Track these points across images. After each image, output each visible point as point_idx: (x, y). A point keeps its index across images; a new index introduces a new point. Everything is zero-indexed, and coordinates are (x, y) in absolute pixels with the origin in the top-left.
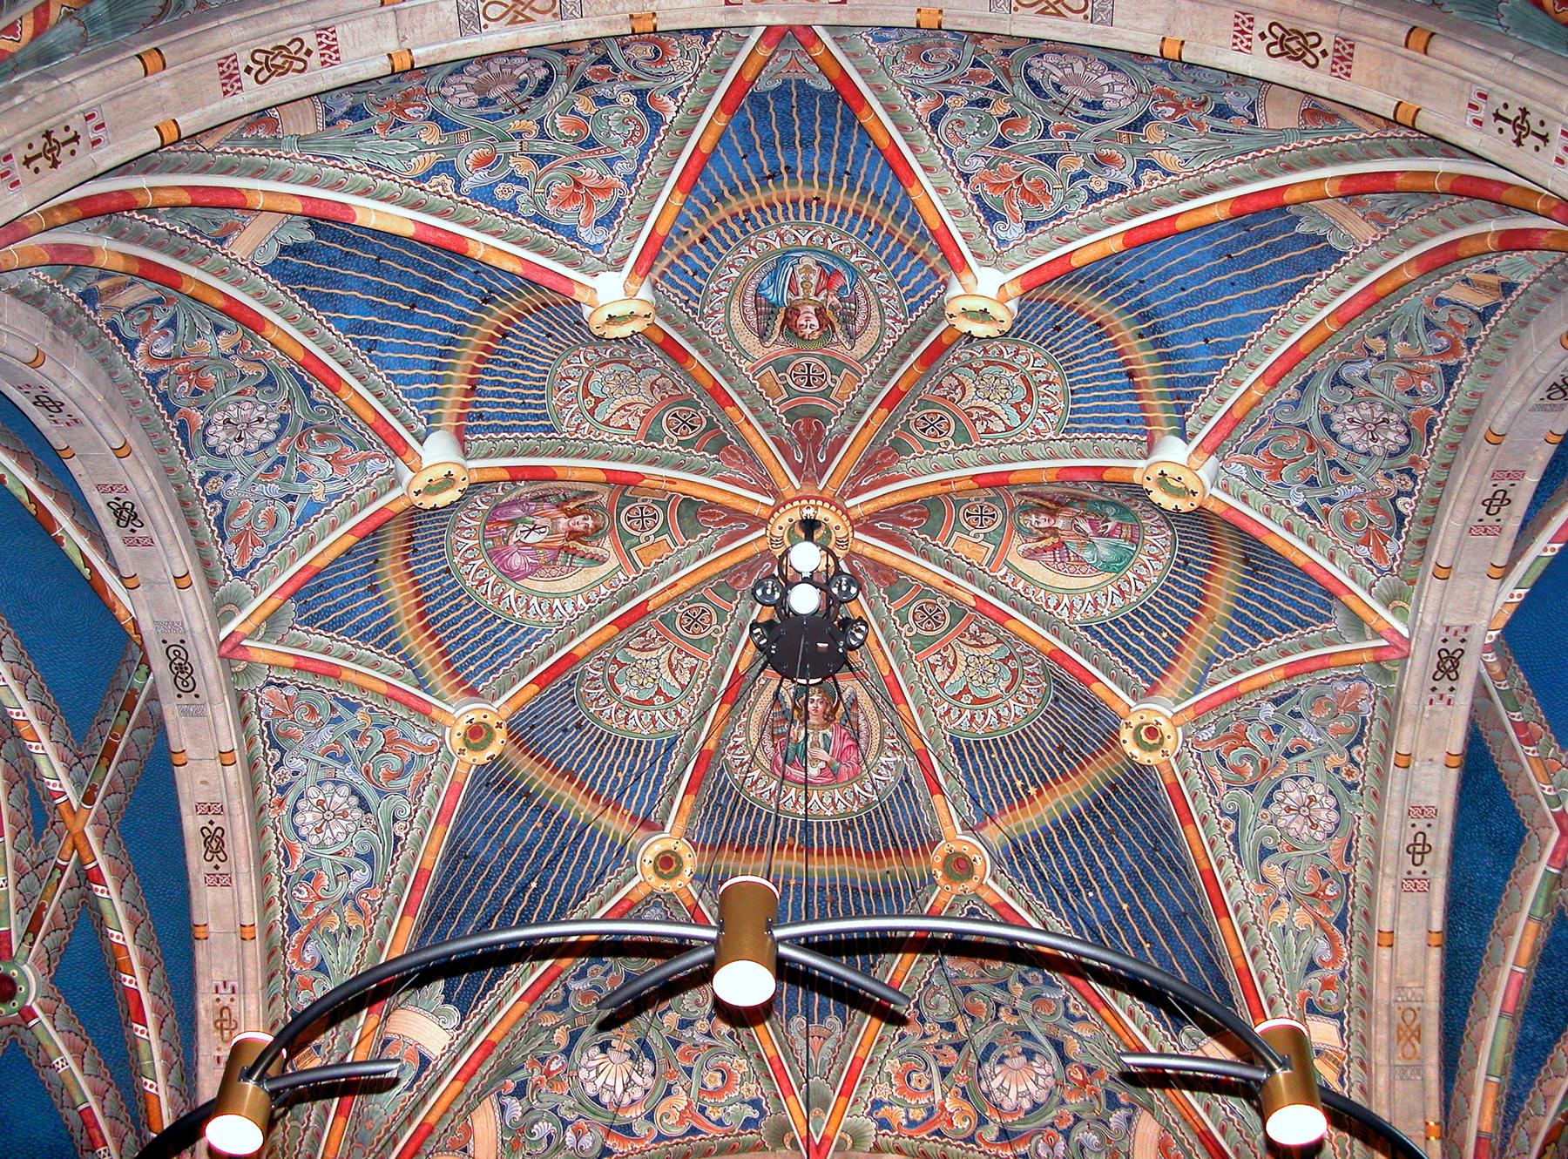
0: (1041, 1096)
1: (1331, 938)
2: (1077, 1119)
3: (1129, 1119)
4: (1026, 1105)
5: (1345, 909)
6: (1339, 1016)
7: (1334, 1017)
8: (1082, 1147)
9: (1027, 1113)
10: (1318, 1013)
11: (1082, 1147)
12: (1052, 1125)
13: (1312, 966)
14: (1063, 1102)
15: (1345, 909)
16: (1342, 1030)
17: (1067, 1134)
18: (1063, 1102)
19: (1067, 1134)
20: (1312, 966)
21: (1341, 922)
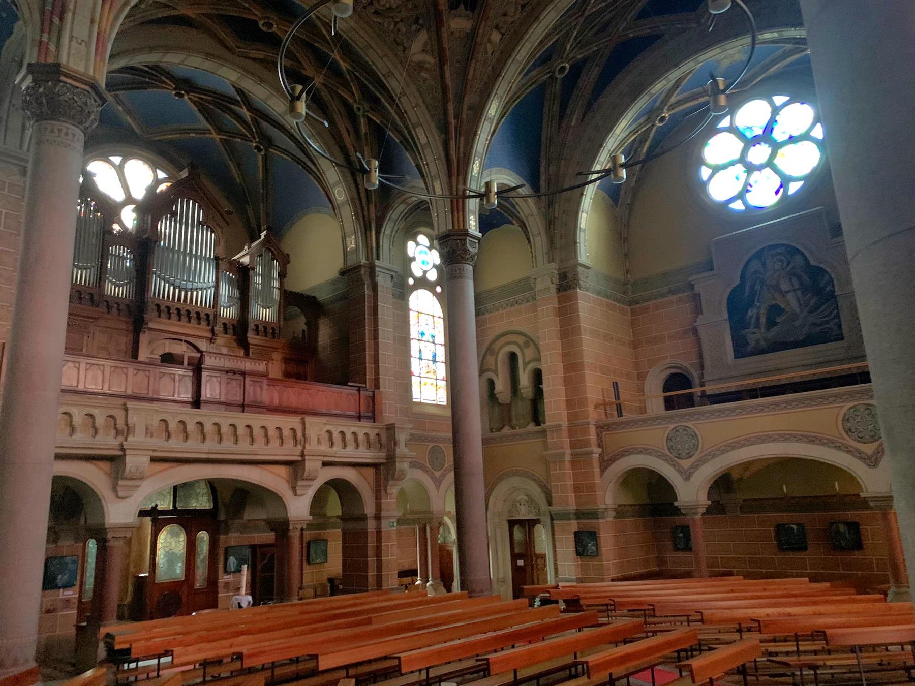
0: (394, 6)
1: (516, 9)
2: (402, 21)
3: (419, 30)
4: (388, 6)
5: (527, 3)
6: (503, 34)
7: (501, 33)
8: (399, 30)
9: (387, 9)
10: (498, 30)
11: (399, 30)
12: (393, 18)
13: (505, 15)
14: (400, 12)
15: (527, 3)
16: (501, 39)
17: (396, 23)
18: (400, 12)
19: (396, 23)
20: (505, 15)
21: (523, 6)
